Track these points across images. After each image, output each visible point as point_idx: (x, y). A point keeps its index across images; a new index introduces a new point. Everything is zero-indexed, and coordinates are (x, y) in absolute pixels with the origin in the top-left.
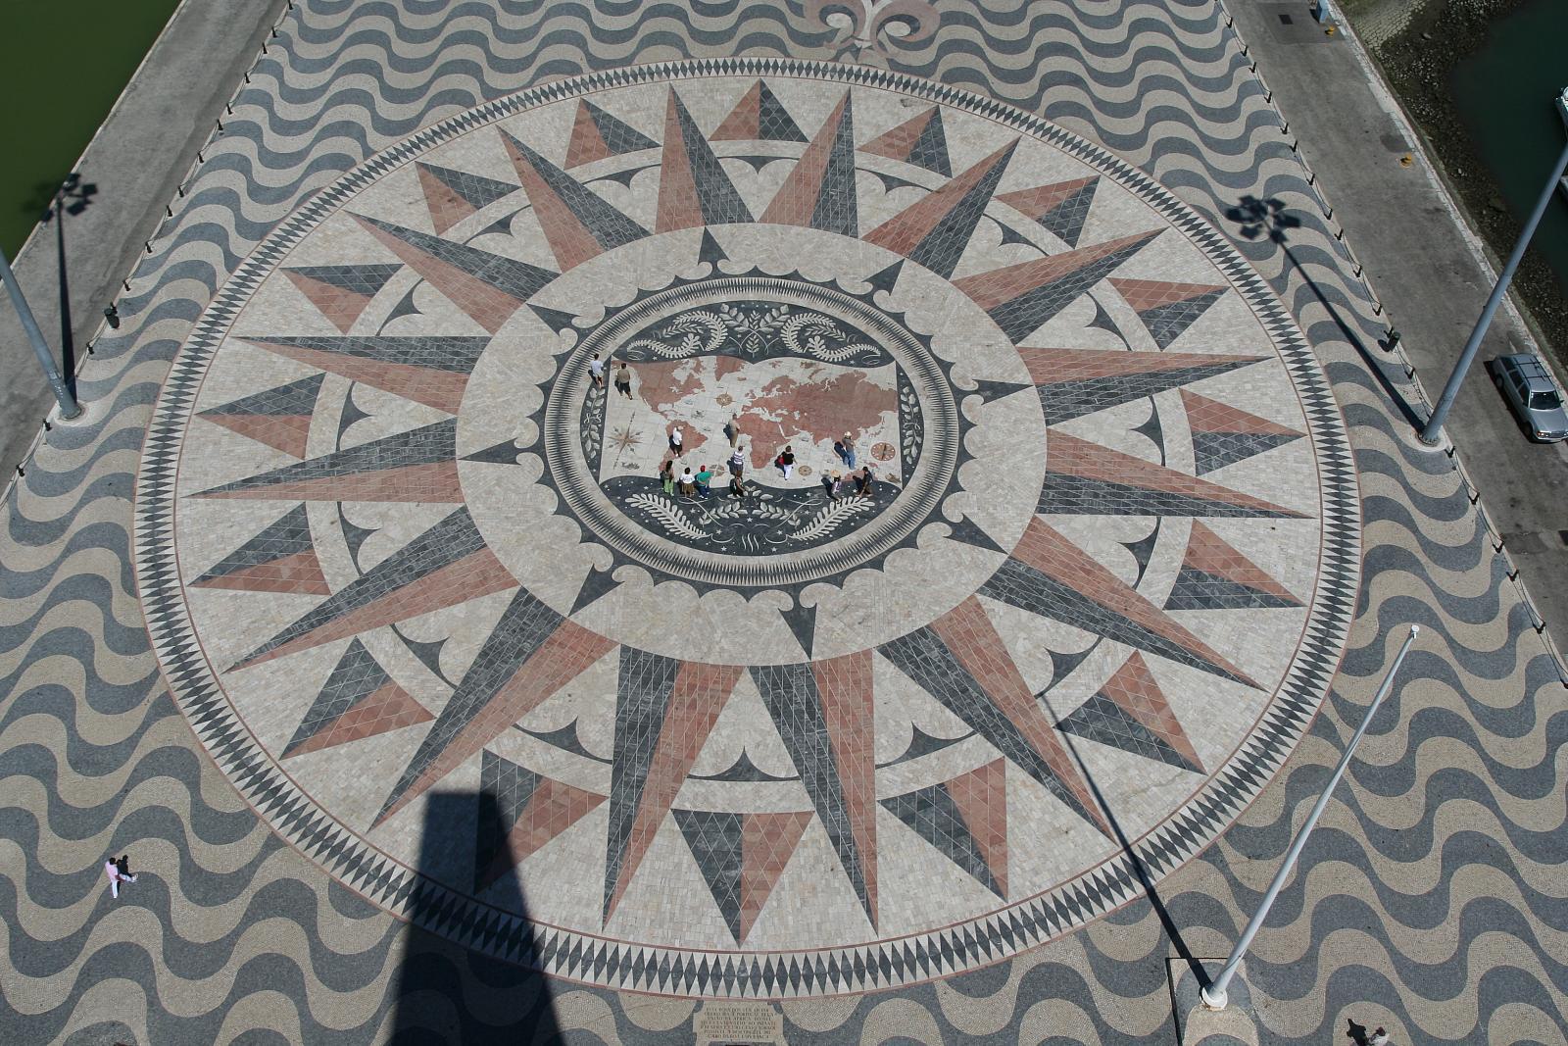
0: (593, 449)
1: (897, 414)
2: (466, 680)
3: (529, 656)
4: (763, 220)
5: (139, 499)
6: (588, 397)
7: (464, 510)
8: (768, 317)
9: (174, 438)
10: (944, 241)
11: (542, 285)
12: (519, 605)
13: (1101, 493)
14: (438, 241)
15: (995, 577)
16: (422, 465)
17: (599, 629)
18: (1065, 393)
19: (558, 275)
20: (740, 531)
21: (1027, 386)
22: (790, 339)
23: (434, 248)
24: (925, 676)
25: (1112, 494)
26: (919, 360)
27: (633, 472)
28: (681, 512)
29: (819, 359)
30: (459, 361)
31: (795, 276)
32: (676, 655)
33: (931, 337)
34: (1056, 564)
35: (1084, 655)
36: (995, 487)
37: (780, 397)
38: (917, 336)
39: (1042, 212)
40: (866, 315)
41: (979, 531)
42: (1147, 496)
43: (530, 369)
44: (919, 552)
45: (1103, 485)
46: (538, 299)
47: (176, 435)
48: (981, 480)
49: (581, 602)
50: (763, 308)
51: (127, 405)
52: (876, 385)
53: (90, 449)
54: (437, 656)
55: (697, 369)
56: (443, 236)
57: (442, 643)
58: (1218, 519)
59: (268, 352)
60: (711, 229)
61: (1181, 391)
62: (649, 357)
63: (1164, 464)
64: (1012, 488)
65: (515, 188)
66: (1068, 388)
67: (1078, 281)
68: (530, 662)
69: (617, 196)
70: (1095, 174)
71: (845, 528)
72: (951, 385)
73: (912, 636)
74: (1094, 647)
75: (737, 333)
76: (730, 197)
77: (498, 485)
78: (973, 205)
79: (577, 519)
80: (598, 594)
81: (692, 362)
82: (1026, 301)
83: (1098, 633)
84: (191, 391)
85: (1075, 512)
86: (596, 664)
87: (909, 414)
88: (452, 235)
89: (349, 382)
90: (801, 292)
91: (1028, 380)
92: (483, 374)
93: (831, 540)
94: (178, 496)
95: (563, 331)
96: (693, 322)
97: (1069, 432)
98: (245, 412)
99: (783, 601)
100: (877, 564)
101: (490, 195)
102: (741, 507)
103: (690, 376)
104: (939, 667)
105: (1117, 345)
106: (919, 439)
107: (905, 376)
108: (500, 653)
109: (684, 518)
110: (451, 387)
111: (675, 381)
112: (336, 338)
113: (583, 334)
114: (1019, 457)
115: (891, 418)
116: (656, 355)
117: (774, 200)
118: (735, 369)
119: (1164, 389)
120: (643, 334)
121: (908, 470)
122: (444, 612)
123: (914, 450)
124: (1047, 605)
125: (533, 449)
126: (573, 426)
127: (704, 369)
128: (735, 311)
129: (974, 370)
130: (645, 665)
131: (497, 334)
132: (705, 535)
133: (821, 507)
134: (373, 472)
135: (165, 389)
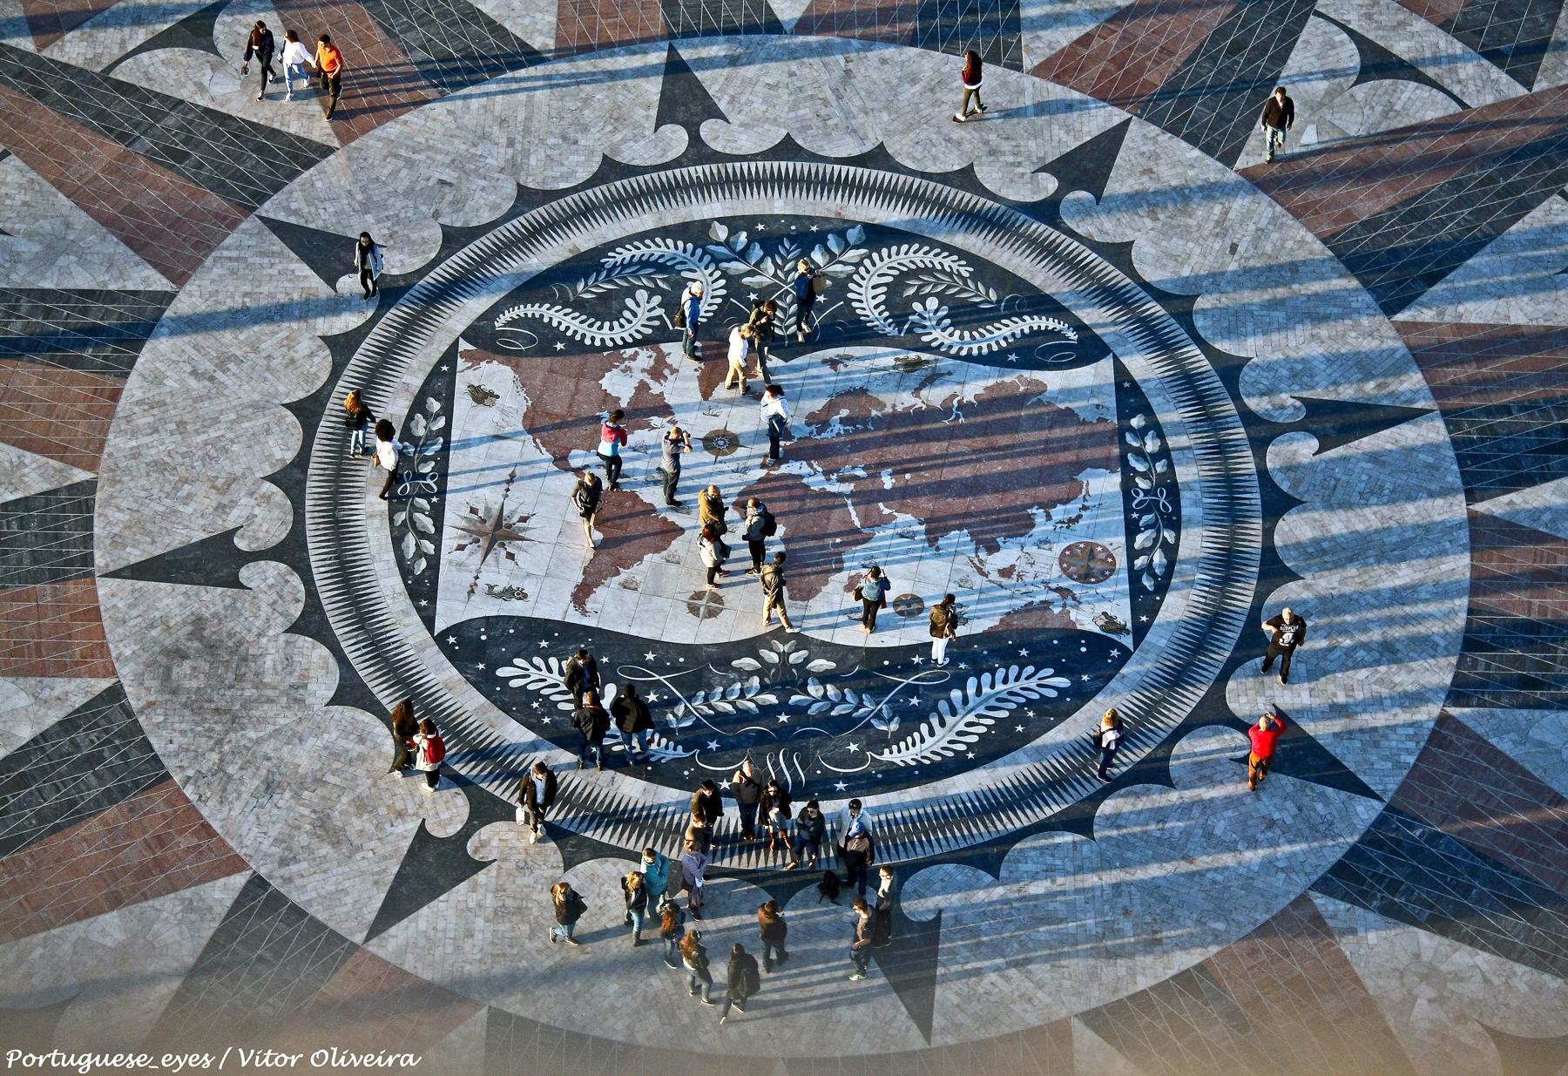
0: (419, 554)
1: (1117, 478)
7: (116, 693)
11: (293, 175)
19: (326, 151)
22: (868, 301)
23: (33, 80)
27: (515, 608)
29: (935, 350)
31: (878, 157)
43: (268, 369)
49: (396, 907)
50: (806, 236)
55: (657, 373)
75: (749, 289)
80: (434, 890)
81: (645, 358)
90: (889, 194)
92: (157, 379)
96: (644, 263)
103: (642, 387)
106: (1169, 535)
116: (561, 336)
121: (1145, 601)
123: (1158, 558)
125: (273, 554)
127: (674, 371)
131: (192, 286)
133: (947, 688)
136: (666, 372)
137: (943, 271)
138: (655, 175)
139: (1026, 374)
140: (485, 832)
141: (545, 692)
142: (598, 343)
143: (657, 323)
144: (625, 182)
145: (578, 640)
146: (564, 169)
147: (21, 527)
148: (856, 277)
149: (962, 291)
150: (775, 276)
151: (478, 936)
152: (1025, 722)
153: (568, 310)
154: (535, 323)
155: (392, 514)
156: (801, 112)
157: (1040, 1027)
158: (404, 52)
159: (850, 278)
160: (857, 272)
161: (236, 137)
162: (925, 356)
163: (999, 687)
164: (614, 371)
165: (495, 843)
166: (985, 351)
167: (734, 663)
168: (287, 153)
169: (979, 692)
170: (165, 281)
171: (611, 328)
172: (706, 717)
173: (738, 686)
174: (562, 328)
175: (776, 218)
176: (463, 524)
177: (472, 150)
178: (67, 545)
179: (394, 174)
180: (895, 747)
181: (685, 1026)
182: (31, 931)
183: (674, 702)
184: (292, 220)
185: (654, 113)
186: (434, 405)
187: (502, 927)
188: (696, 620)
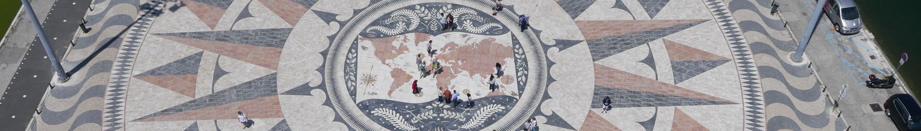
0: (352, 85)
1: (513, 59)
5: (104, 124)
6: (347, 58)
7: (284, 121)
9: (121, 90)
16: (260, 98)
18: (602, 44)
21: (582, 41)
25: (630, 96)
28: (401, 117)
29: (470, 32)
30: (276, 42)
36: (568, 95)
41: (561, 120)
42: (649, 96)
43: (315, 44)
45: (626, 91)
47: (123, 88)
48: (560, 92)
51: (95, 74)
53: (76, 98)
55: (405, 41)
58: (688, 107)
59: (171, 41)
61: (664, 40)
62: (378, 35)
63: (657, 79)
64: (577, 96)
71: (489, 122)
72: (541, 42)
75: (425, 20)
77: (302, 106)
81: (402, 37)
84: (130, 64)
87: (519, 59)
89: (217, 55)
91: (582, 38)
93: (483, 128)
94: (126, 121)
95: (332, 23)
96: (401, 16)
97: (605, 65)
98: (160, 74)
102: (434, 113)
105: (628, 17)
106: (526, 72)
107: (516, 39)
109: (403, 120)
110: (273, 56)
111: (394, 48)
112: (208, 32)
113: (342, 24)
114: (580, 79)
116: (382, 33)
119: (654, 39)
120: (374, 23)
121: (521, 89)
123: (524, 77)
125: (319, 87)
126: (340, 74)
127: (409, 40)
128: (423, 9)
129: (553, 34)
132: (415, 129)
134: (233, 103)
135: (116, 63)
136: (407, 40)
142: (391, 34)
147: (261, 84)
150: (431, 17)
154: (376, 31)
155: (345, 76)
162: (467, 34)
163: (488, 109)
167: (427, 107)
169: (484, 111)
170: (290, 25)
172: (420, 120)
173: (428, 112)
176: (362, 78)
183: (413, 117)
184: (319, 10)
186: (353, 51)
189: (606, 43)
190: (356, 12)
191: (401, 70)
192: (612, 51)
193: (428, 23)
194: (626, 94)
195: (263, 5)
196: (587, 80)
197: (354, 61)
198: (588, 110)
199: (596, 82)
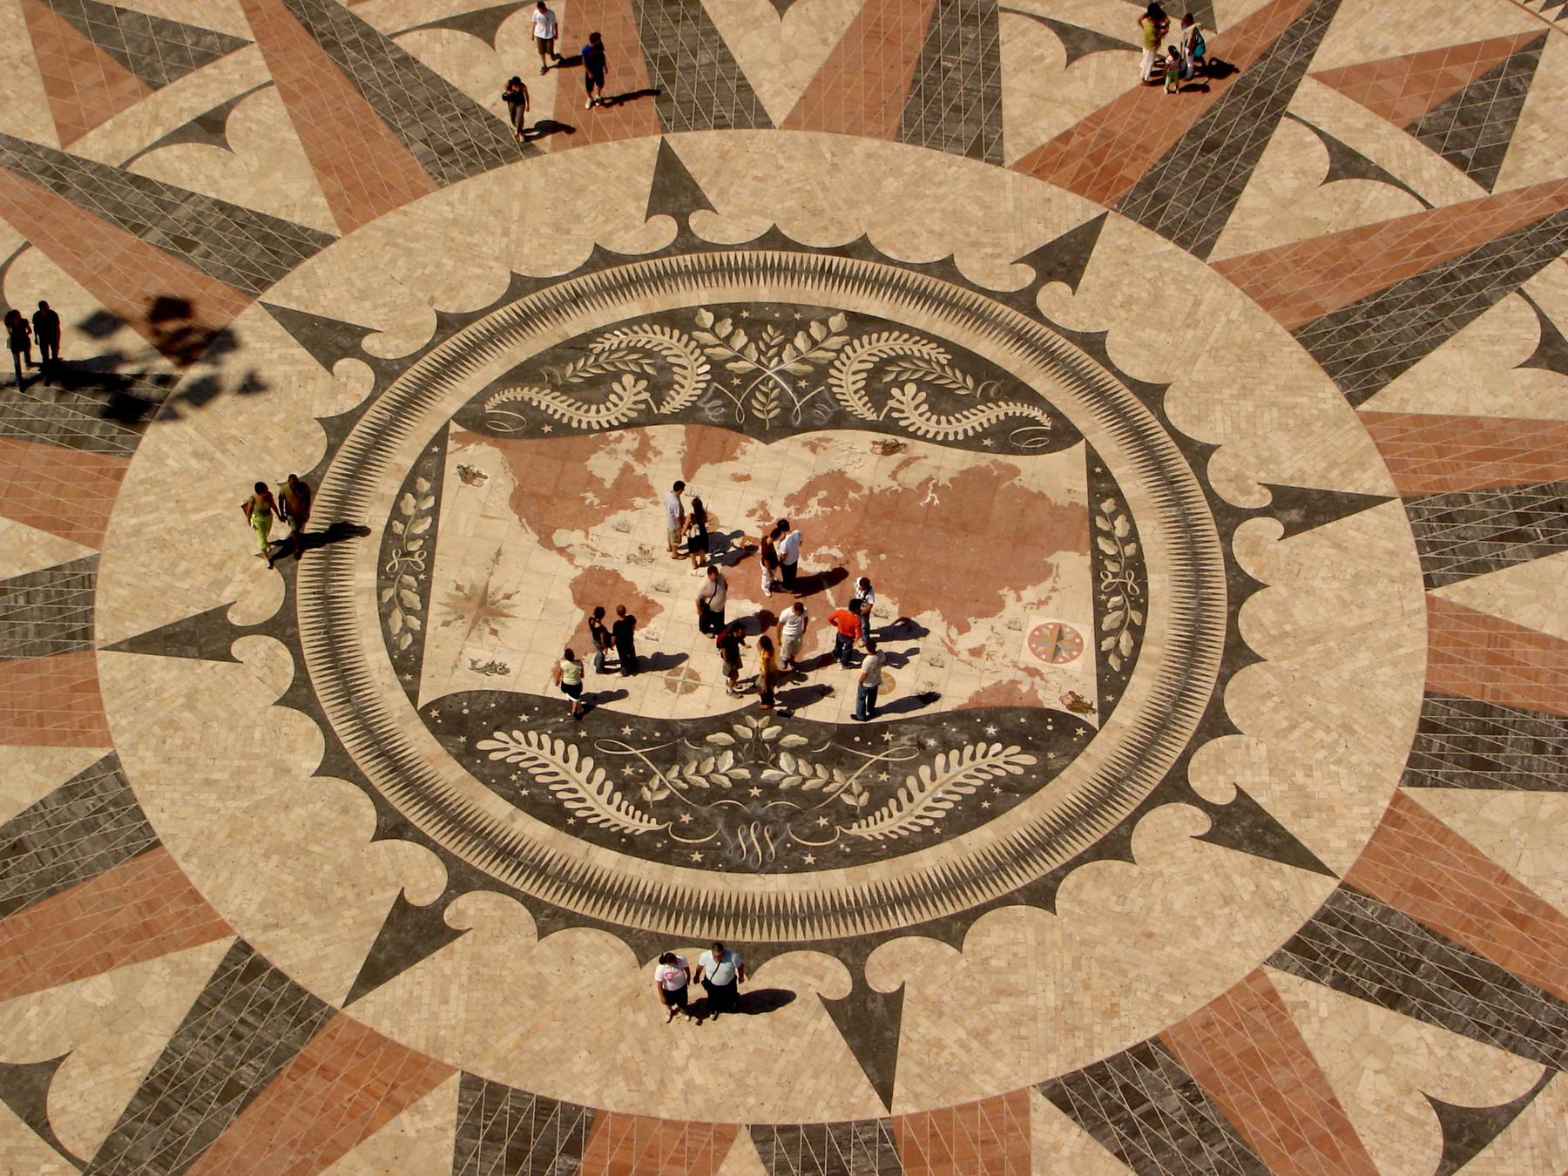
0: (406, 629)
1: (1087, 560)
2: (107, 1150)
3: (252, 1096)
4: (791, 122)
7: (111, 762)
8: (800, 341)
10: (1196, 173)
11: (295, 262)
12: (231, 979)
13: (1551, 742)
14: (64, 160)
15: (1308, 929)
17: (413, 1037)
18: (1469, 517)
19: (328, 240)
20: (735, 819)
22: (848, 385)
23: (55, 175)
24: (1148, 1152)
26: (1137, 436)
27: (494, 682)
28: (601, 774)
29: (914, 436)
31: (862, 248)
32: (584, 1095)
33: (1164, 388)
34: (1448, 903)
35: (1512, 1110)
36: (1307, 725)
37: (828, 519)
38: (1135, 386)
39: (1418, 110)
40: (1020, 338)
41: (1271, 826)
43: (265, 449)
44: (1134, 870)
45: (1556, 724)
46: (289, 292)
49: (373, 975)
50: (791, 321)
52: (1041, 496)
54: (42, 1095)
55: (641, 454)
56: (76, 150)
57: (54, 1065)
60: (673, 140)
62: (535, 425)
64: (1346, 728)
65: (237, 44)
66: (1477, 505)
67: (1497, 264)
68: (253, 1111)
69: (465, 65)
70: (1537, 26)
72: (1210, 495)
73: (1119, 1060)
74: (1536, 1091)
75: (732, 374)
76: (719, 71)
77: (190, 705)
78: (1261, 93)
79: (366, 786)
81: (630, 439)
82: (1381, 308)
83: (1544, 1061)
85: (1490, 785)
86: (404, 1116)
87: (1114, 559)
88: (95, 147)
90: (874, 284)
92: (160, 459)
93: (937, 840)
95: (342, 365)
97: (1478, 604)
99: (828, 978)
100: (1042, 895)
101: (183, 59)
102: (737, 762)
103: (627, 469)
104: (1181, 1133)
106: (1136, 616)
107: (1107, 475)
108: (186, 1088)
109: (609, 786)
110: (87, 486)
111: (592, 481)
113: (385, 372)
114: (1364, 658)
115: (1073, 566)
116: (549, 420)
117: (817, 82)
118: (726, 454)
120: (521, 375)
121: (1112, 683)
122: (61, 995)
123: (1125, 641)
124: (1428, 996)
127: (657, 453)
128: (726, 327)
130: (514, 1120)
133: (915, 765)
136: (650, 455)
137: (922, 359)
138: (644, 264)
139: (1001, 458)
140: (463, 901)
141: (522, 765)
142: (584, 426)
143: (643, 406)
144: (615, 270)
145: (557, 714)
146: (557, 258)
147: (28, 602)
148: (837, 363)
149: (940, 377)
150: (758, 361)
151: (453, 1003)
152: (991, 797)
153: (556, 394)
154: (524, 406)
156: (787, 204)
157: (999, 1097)
158: (406, 146)
159: (831, 363)
160: (838, 358)
161: (243, 227)
162: (901, 440)
164: (601, 453)
165: (471, 912)
166: (961, 437)
167: (710, 738)
168: (290, 242)
171: (598, 411)
172: (681, 790)
174: (550, 411)
175: (760, 306)
177: (469, 239)
178: (71, 619)
179: (393, 261)
180: (863, 822)
181: (652, 1093)
182: (28, 989)
183: (649, 775)
184: (293, 306)
185: (645, 204)
186: (424, 485)
187: (478, 994)
188: (673, 696)
189: (1484, 514)
190: (447, 324)
191: (615, 575)
192: (1510, 547)
193: (742, 387)
194: (1556, 733)
195: (63, 274)
196: (1395, 664)
197: (422, 527)
198: (1391, 792)
199: (1430, 672)
